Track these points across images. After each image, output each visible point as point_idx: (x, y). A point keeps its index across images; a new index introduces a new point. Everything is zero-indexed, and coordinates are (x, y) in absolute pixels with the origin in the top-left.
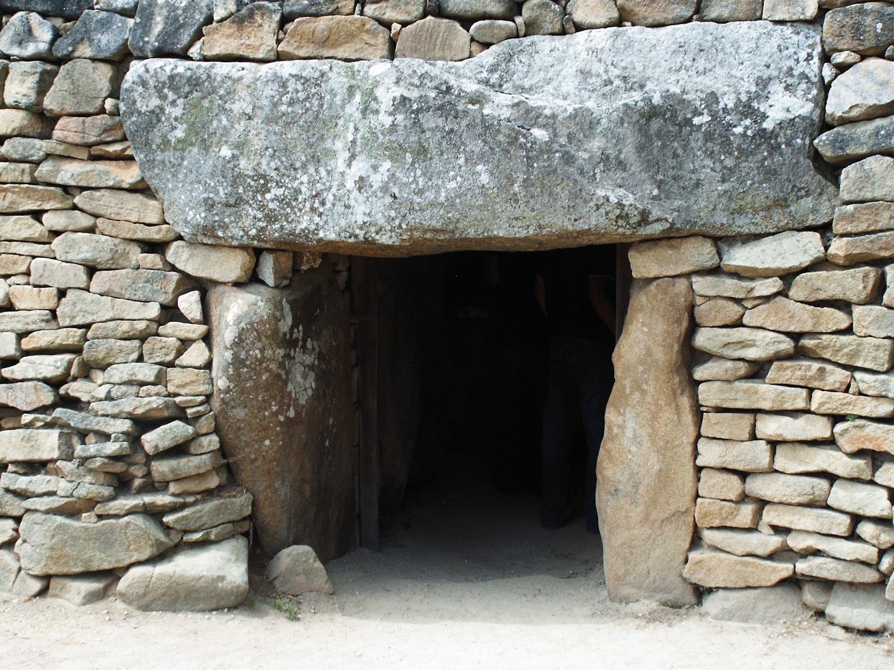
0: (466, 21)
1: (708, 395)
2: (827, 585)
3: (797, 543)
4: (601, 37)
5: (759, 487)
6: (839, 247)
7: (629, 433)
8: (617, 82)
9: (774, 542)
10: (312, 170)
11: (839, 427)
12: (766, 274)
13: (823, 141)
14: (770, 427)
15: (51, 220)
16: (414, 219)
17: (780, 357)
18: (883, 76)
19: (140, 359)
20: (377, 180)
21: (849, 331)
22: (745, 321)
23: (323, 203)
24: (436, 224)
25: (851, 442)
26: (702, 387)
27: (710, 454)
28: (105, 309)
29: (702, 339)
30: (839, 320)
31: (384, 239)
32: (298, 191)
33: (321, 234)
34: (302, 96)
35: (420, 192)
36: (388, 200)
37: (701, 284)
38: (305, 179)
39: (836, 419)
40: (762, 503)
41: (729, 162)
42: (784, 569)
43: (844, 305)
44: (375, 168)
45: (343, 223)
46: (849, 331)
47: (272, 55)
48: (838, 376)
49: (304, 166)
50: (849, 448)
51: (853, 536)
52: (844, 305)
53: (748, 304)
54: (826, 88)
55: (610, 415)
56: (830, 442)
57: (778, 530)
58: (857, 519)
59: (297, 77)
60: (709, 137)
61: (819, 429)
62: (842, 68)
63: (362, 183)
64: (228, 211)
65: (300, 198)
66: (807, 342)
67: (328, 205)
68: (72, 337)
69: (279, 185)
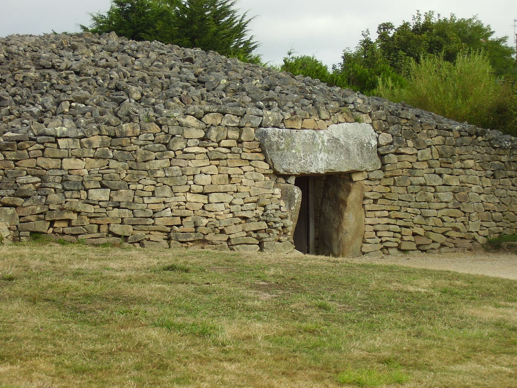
0: (324, 120)
1: (367, 207)
2: (387, 248)
3: (384, 239)
4: (345, 124)
5: (378, 227)
6: (388, 174)
7: (350, 217)
8: (350, 136)
9: (380, 240)
10: (310, 156)
11: (391, 213)
12: (375, 180)
13: (380, 150)
14: (378, 214)
15: (245, 169)
16: (330, 167)
17: (381, 198)
18: (387, 137)
19: (272, 204)
20: (325, 158)
21: (390, 192)
22: (373, 190)
23: (312, 164)
24: (333, 169)
25: (393, 216)
26: (366, 205)
27: (369, 221)
28: (262, 191)
29: (367, 194)
30: (388, 189)
31: (322, 172)
32: (307, 161)
33: (312, 171)
34: (309, 138)
35: (332, 161)
36: (326, 163)
37: (366, 182)
38: (309, 158)
39: (389, 211)
40: (376, 231)
41: (369, 155)
42: (382, 246)
43: (388, 186)
44: (324, 155)
45: (316, 168)
46: (390, 192)
47: (300, 128)
48: (390, 202)
49: (309, 155)
50: (393, 218)
51: (394, 237)
52: (388, 186)
53: (373, 186)
54: (377, 138)
55: (346, 214)
56: (389, 217)
57: (380, 237)
58: (395, 232)
59: (309, 134)
60: (367, 149)
61: (386, 213)
62: (379, 134)
63: (322, 159)
64: (293, 165)
65: (308, 162)
66: (384, 195)
67: (314, 164)
68: (255, 199)
69: (304, 159)
